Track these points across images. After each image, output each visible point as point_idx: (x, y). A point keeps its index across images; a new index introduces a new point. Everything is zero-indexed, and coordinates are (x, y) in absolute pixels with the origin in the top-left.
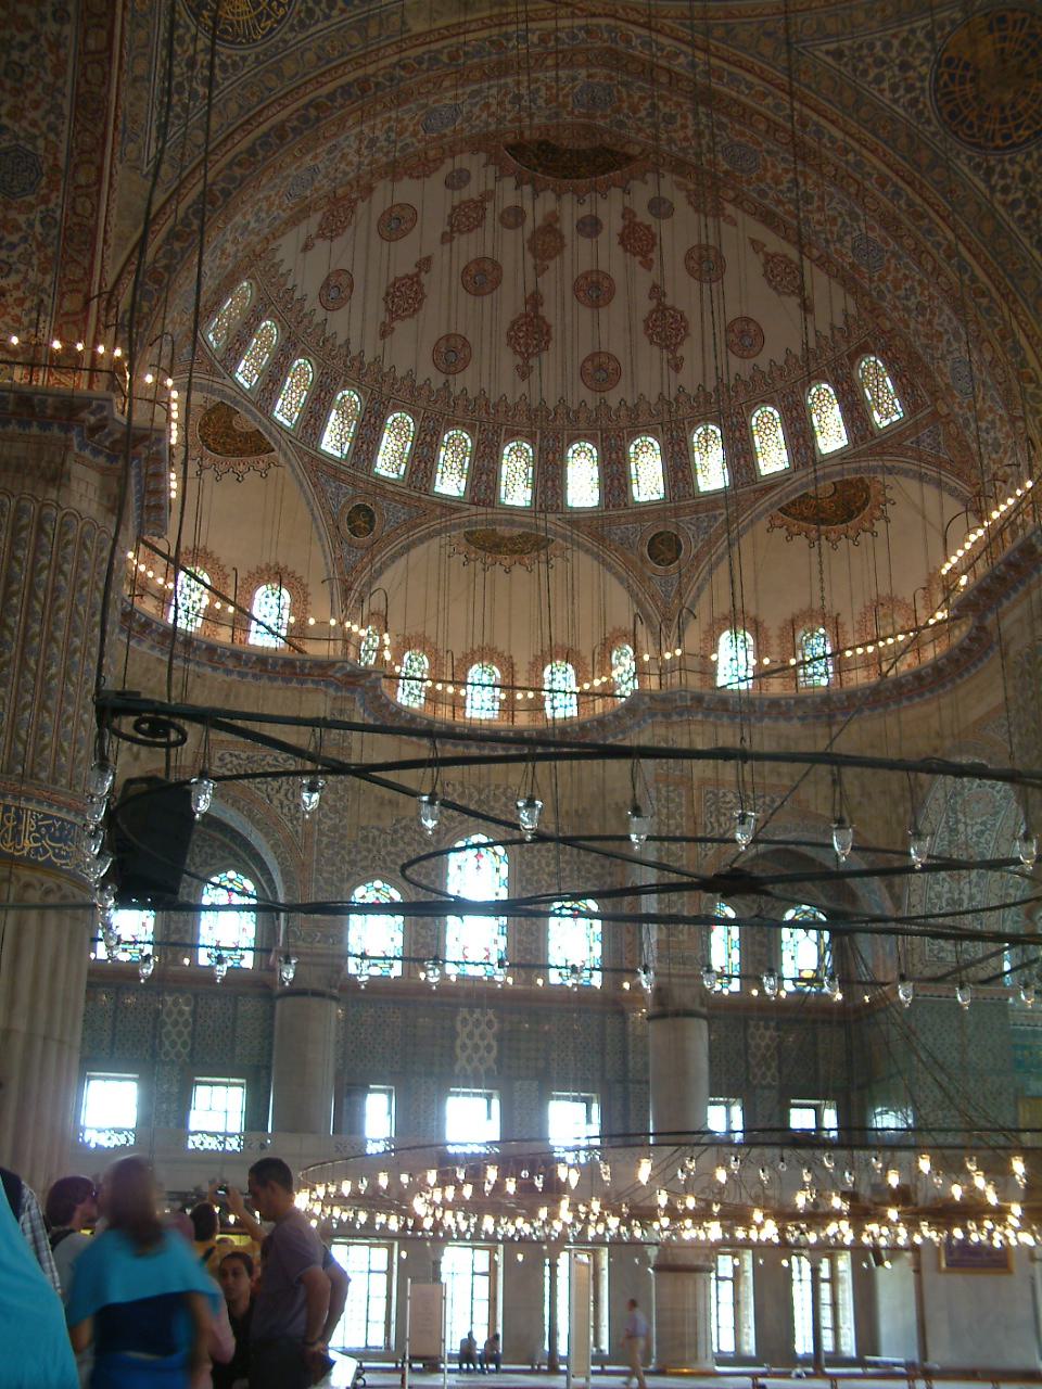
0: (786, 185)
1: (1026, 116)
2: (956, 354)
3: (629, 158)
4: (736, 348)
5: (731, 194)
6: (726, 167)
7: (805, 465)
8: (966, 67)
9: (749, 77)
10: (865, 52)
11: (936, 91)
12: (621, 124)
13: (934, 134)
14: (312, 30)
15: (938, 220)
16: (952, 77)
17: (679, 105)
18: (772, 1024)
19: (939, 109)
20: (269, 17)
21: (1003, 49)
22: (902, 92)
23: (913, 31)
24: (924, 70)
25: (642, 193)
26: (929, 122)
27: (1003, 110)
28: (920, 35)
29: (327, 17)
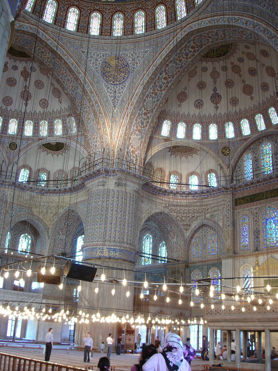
2: (92, 124)
3: (29, 57)
4: (41, 105)
5: (51, 73)
7: (51, 136)
9: (63, 50)
11: (102, 67)
15: (95, 95)
16: (106, 66)
18: (14, 260)
23: (100, 53)
24: (100, 62)
25: (29, 65)
26: (99, 73)
27: (114, 76)
28: (101, 55)
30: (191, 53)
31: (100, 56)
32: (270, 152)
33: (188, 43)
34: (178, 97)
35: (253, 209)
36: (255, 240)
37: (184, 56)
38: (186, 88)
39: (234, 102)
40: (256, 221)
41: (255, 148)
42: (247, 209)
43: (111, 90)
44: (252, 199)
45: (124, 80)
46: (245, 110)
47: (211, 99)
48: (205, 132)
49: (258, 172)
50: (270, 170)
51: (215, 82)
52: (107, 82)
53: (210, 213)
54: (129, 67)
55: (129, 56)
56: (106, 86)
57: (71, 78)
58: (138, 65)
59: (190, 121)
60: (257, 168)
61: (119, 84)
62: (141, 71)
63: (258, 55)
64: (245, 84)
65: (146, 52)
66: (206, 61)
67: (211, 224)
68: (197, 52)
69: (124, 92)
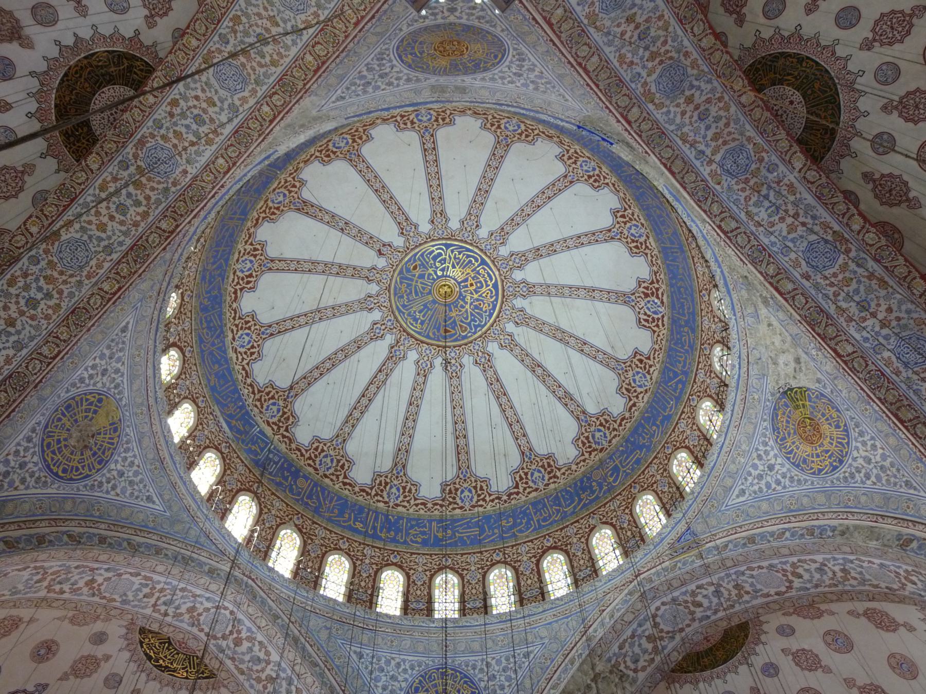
0: (45, 287)
1: (59, 456)
6: (64, 237)
8: (95, 412)
10: (120, 346)
11: (85, 394)
12: (124, 165)
13: (59, 397)
14: (372, 56)
16: (91, 404)
17: (136, 224)
19: (73, 398)
20: (409, 44)
21: (100, 434)
22: (91, 372)
24: (99, 385)
27: (65, 440)
28: (118, 381)
29: (367, 65)
31: (115, 376)
33: (208, 599)
37: (163, 599)
43: (26, 449)
45: (60, 474)
52: (46, 427)
54: (98, 470)
55: (128, 455)
56: (33, 430)
57: (47, 317)
58: (113, 493)
61: (48, 466)
62: (98, 510)
65: (149, 499)
69: (29, 492)
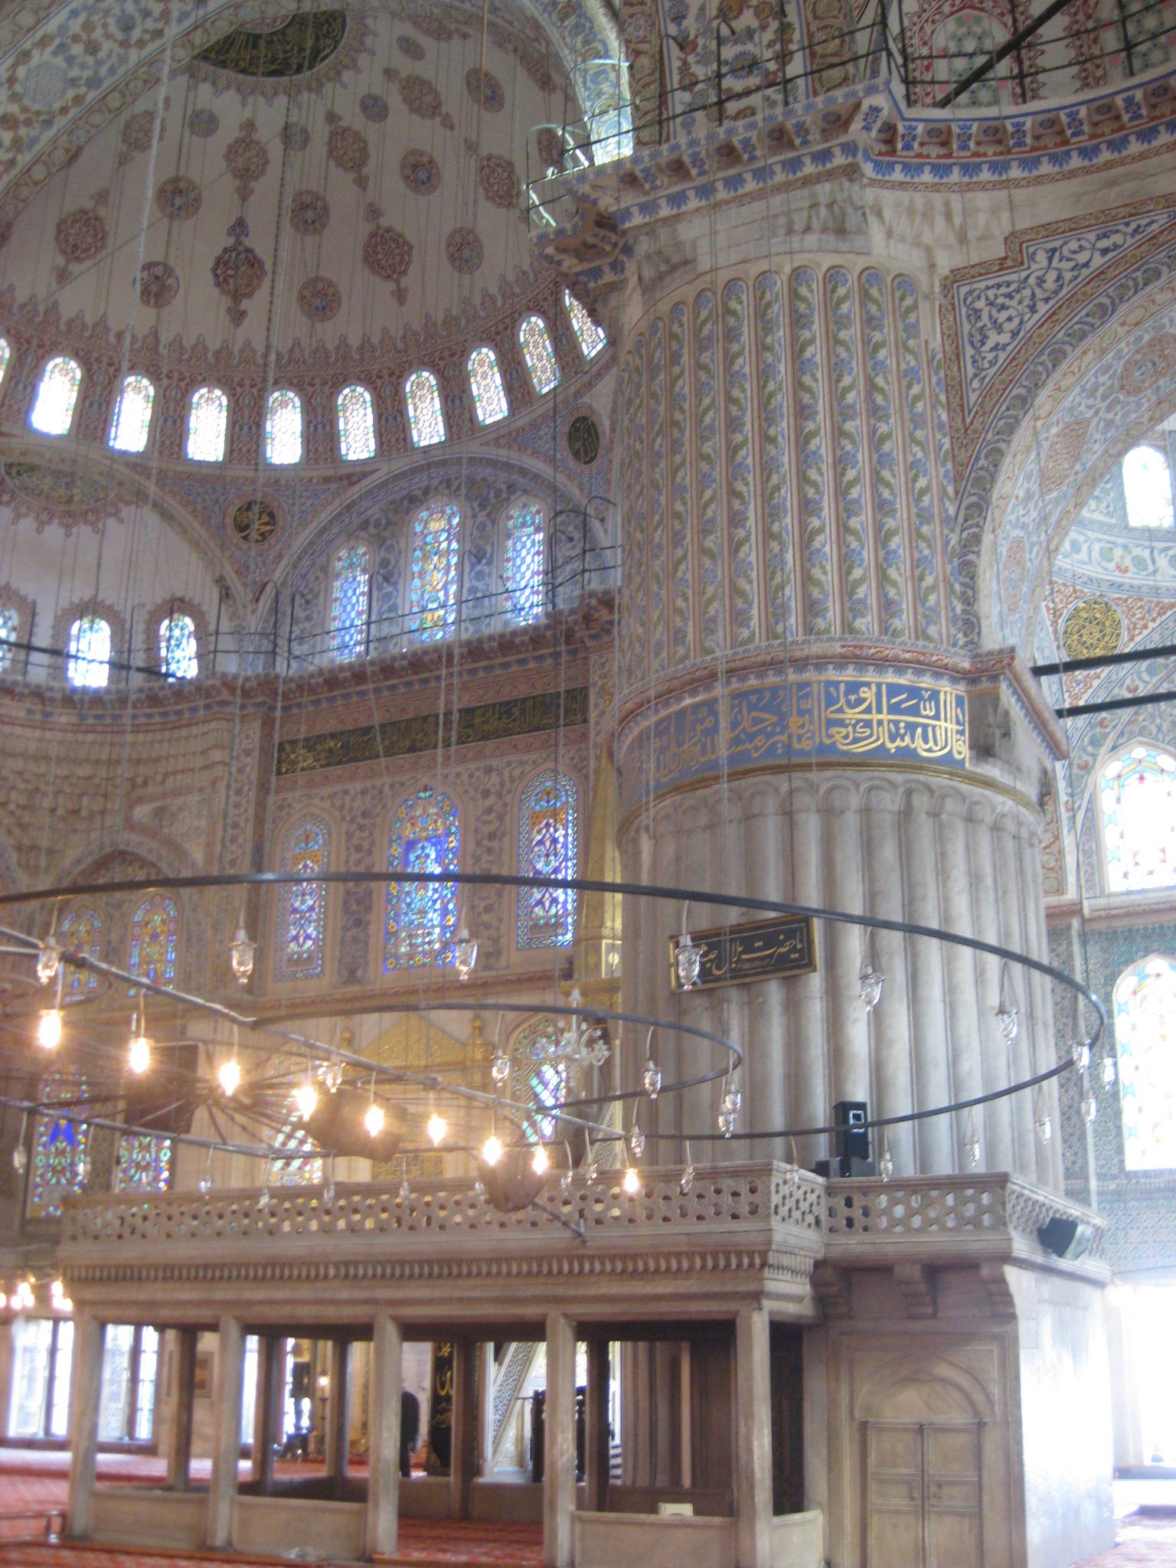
30: (150, 24)
32: (454, 545)
34: (61, 231)
35: (352, 792)
36: (349, 934)
37: (113, 28)
38: (102, 197)
39: (319, 299)
40: (358, 848)
41: (389, 524)
42: (326, 791)
44: (350, 749)
46: (366, 346)
47: (214, 270)
48: (170, 424)
49: (386, 629)
50: (445, 625)
51: (244, 193)
53: (152, 800)
59: (105, 360)
60: (390, 610)
63: (453, 93)
64: (379, 227)
66: (214, 83)
67: (151, 851)
68: (180, 21)
